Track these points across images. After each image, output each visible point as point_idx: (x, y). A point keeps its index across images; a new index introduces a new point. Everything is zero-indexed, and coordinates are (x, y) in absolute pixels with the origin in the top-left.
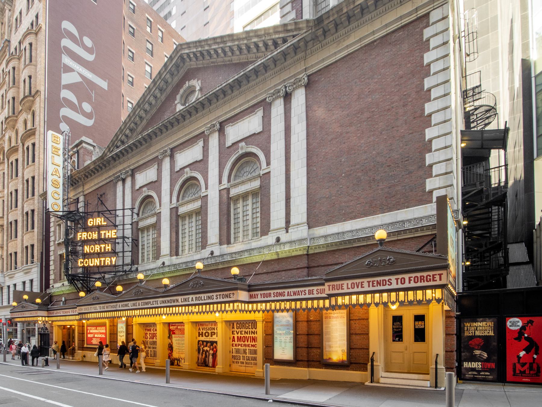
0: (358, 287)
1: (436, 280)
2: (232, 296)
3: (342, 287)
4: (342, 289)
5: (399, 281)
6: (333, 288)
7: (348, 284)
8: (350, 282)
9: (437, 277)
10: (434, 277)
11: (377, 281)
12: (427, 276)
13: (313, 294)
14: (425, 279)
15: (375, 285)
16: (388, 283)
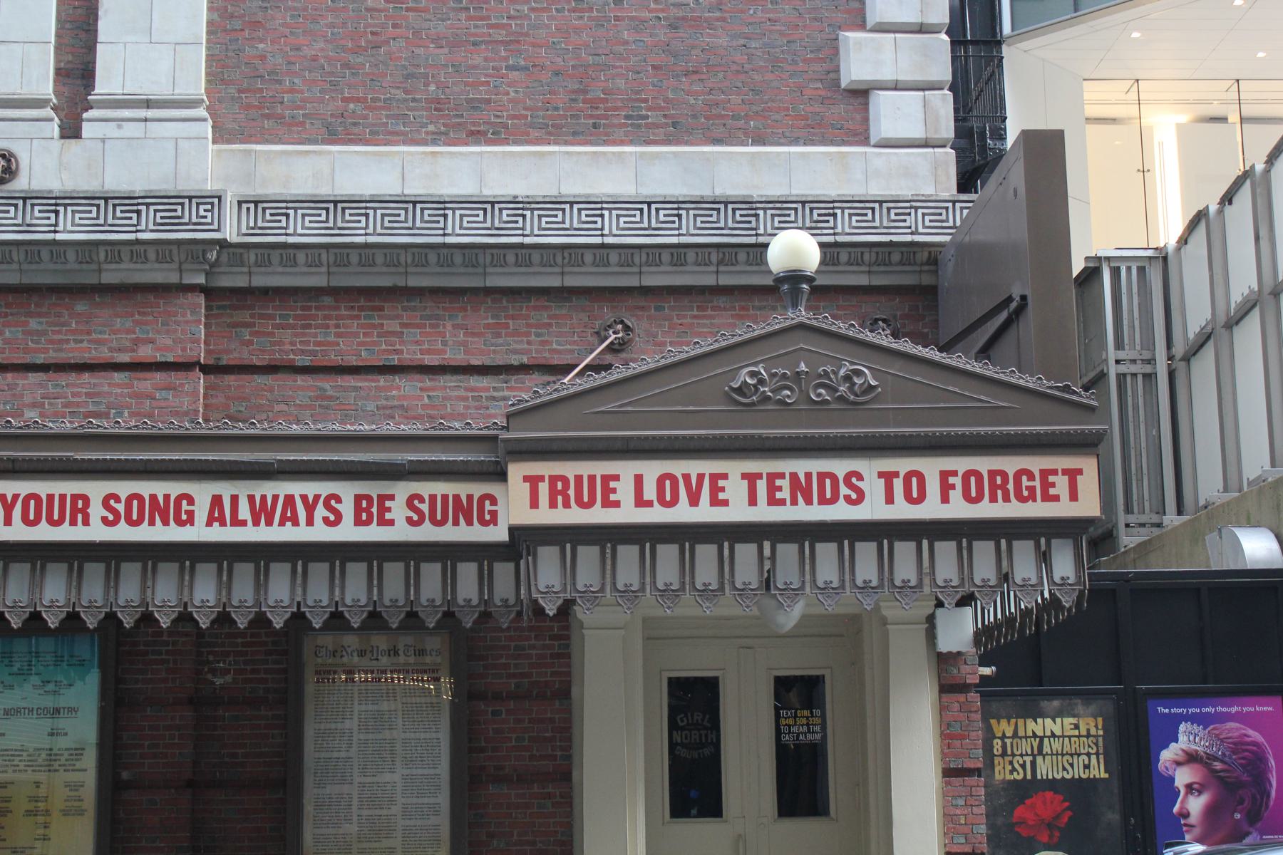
0: (694, 501)
1: (1056, 498)
3: (607, 491)
4: (607, 503)
5: (898, 484)
6: (553, 494)
7: (639, 480)
8: (652, 470)
9: (1061, 485)
10: (1046, 485)
11: (794, 476)
12: (1019, 474)
13: (383, 522)
14: (1011, 486)
15: (784, 494)
16: (844, 490)
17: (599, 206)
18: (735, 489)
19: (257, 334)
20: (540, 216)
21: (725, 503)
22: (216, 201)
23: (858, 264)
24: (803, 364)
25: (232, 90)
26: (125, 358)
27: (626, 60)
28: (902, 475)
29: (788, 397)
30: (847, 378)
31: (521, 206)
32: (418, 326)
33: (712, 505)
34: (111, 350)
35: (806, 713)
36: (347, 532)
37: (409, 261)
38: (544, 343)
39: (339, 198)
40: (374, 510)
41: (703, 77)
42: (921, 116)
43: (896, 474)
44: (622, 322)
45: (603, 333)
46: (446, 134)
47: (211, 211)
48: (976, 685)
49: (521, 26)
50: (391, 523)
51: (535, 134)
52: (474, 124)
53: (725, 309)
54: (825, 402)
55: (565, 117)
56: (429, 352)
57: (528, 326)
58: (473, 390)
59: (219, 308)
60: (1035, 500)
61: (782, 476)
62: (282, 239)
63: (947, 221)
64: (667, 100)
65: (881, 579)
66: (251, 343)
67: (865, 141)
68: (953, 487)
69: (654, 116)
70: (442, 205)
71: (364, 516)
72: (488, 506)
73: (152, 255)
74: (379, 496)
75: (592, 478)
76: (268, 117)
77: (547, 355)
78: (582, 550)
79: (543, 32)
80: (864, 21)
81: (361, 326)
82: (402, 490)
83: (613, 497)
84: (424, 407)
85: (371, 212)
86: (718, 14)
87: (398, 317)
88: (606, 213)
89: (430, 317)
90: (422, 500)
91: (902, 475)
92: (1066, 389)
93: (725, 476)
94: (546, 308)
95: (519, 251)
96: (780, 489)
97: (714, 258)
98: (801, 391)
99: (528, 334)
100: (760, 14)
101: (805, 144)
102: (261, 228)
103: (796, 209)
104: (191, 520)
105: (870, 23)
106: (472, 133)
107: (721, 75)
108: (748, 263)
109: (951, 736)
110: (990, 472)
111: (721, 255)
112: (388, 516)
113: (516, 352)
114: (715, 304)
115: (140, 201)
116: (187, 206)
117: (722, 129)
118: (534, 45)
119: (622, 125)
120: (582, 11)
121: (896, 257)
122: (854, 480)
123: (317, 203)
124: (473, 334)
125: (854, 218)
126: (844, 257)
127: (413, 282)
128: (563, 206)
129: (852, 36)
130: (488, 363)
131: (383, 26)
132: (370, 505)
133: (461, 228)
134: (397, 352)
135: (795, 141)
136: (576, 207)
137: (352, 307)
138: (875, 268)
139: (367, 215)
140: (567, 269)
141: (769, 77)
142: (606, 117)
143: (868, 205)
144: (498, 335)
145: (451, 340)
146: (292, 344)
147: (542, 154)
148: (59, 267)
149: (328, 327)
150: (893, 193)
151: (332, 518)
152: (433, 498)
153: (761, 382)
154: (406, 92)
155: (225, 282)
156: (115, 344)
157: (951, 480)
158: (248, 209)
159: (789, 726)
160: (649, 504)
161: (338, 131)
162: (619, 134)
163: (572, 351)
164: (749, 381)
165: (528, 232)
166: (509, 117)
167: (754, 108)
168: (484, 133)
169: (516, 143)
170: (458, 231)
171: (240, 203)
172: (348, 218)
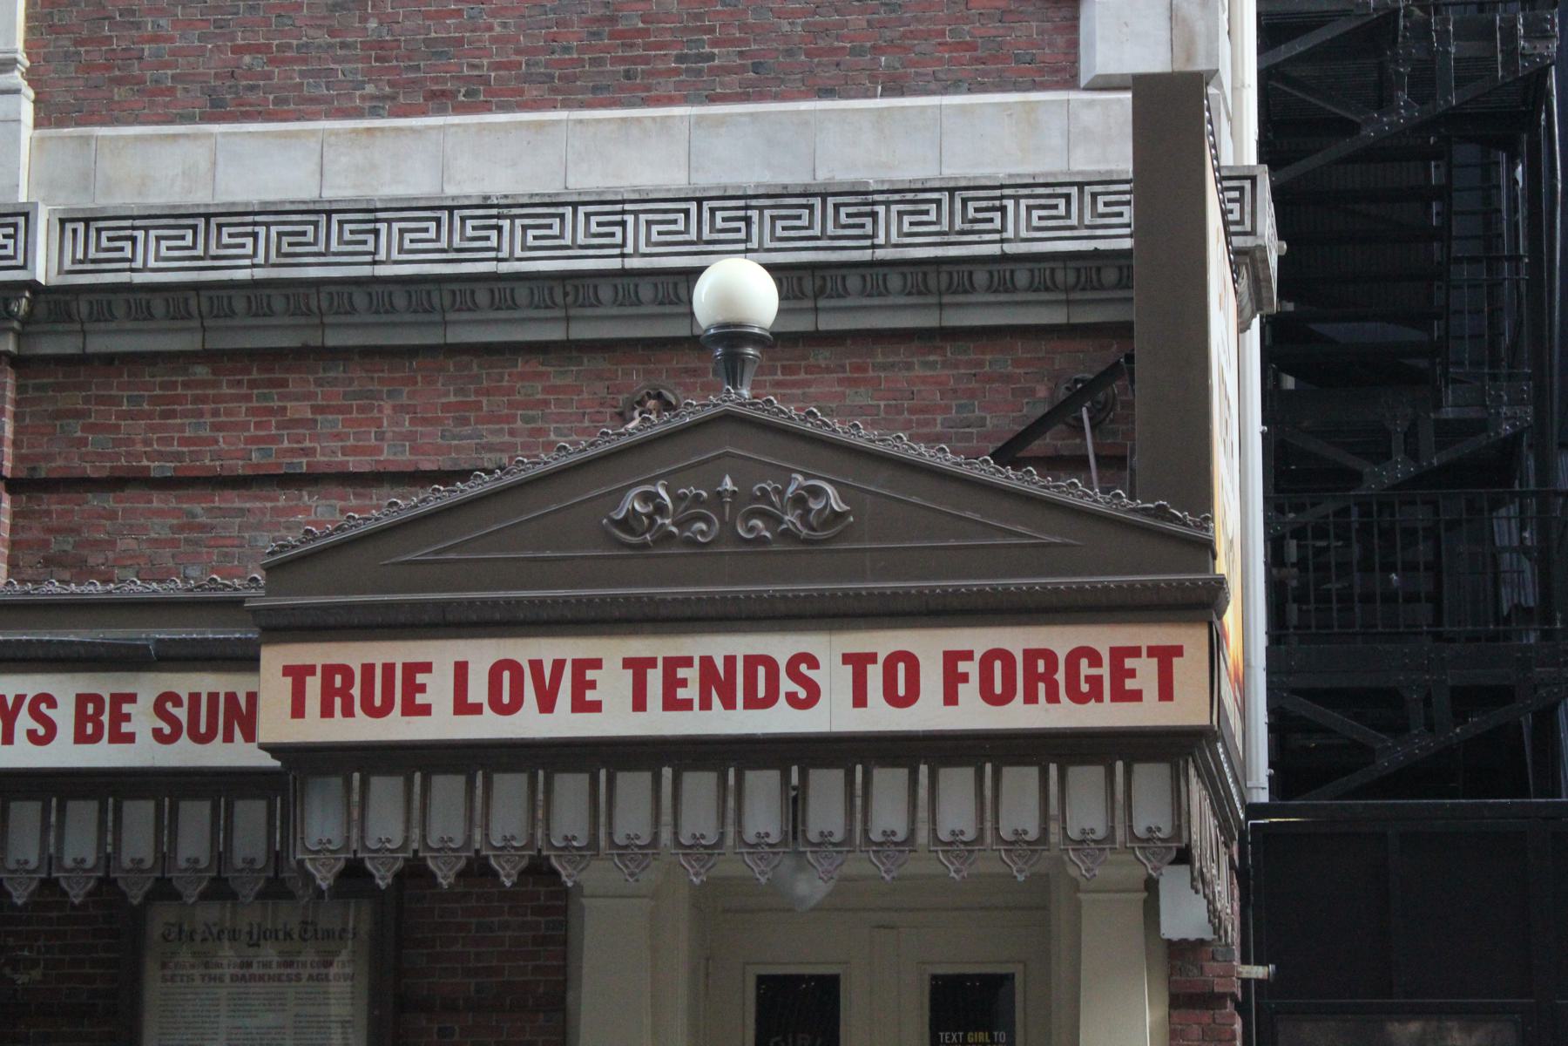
0: (547, 703)
1: (1136, 696)
3: (412, 688)
4: (411, 709)
5: (875, 674)
7: (461, 670)
8: (482, 654)
9: (1145, 673)
10: (1120, 673)
11: (707, 662)
12: (1074, 657)
13: (119, 737)
14: (1060, 677)
15: (691, 692)
16: (786, 685)
17: (618, 207)
18: (612, 685)
20: (525, 228)
21: (596, 707)
22: (21, 221)
23: (1047, 289)
25: (66, 42)
28: (881, 660)
29: (702, 533)
30: (799, 501)
31: (494, 212)
32: (339, 410)
33: (574, 710)
36: (64, 753)
37: (325, 305)
39: (212, 210)
40: (105, 718)
42: (1165, 35)
43: (872, 658)
44: (659, 396)
45: (628, 415)
46: (393, 98)
47: (14, 236)
50: (130, 738)
51: (532, 92)
52: (436, 80)
53: (828, 370)
54: (760, 540)
55: (580, 62)
56: (355, 451)
57: (511, 405)
59: (37, 388)
60: (1100, 699)
61: (687, 662)
62: (124, 278)
64: (743, 27)
65: (850, 831)
66: (83, 442)
67: (1069, 79)
68: (965, 678)
69: (723, 56)
70: (370, 215)
71: (90, 729)
74: (113, 696)
76: (119, 82)
78: (440, 782)
81: (252, 412)
82: (148, 686)
83: (420, 699)
87: (309, 396)
88: (630, 219)
90: (178, 702)
91: (881, 660)
92: (1161, 512)
93: (596, 664)
94: (541, 375)
95: (496, 286)
96: (683, 683)
98: (722, 521)
101: (970, 91)
102: (94, 261)
103: (938, 202)
106: (432, 96)
108: (864, 293)
110: (1027, 652)
111: (818, 282)
112: (126, 728)
113: (490, 448)
114: (812, 361)
117: (834, 71)
122: (803, 668)
125: (1036, 213)
126: (1022, 278)
127: (333, 339)
128: (561, 210)
132: (99, 710)
133: (401, 251)
134: (305, 452)
136: (582, 210)
137: (239, 382)
138: (1077, 296)
139: (255, 235)
140: (572, 312)
142: (646, 60)
143: (1059, 190)
144: (464, 421)
146: (147, 442)
147: (541, 125)
149: (201, 414)
151: (41, 731)
153: (661, 509)
154: (332, 33)
155: (47, 347)
157: (963, 667)
158: (75, 231)
160: (476, 709)
161: (225, 103)
162: (667, 86)
164: (637, 507)
165: (505, 254)
166: (497, 66)
167: (888, 33)
168: (453, 95)
169: (504, 108)
170: (395, 256)
171: (62, 222)
172: (226, 240)
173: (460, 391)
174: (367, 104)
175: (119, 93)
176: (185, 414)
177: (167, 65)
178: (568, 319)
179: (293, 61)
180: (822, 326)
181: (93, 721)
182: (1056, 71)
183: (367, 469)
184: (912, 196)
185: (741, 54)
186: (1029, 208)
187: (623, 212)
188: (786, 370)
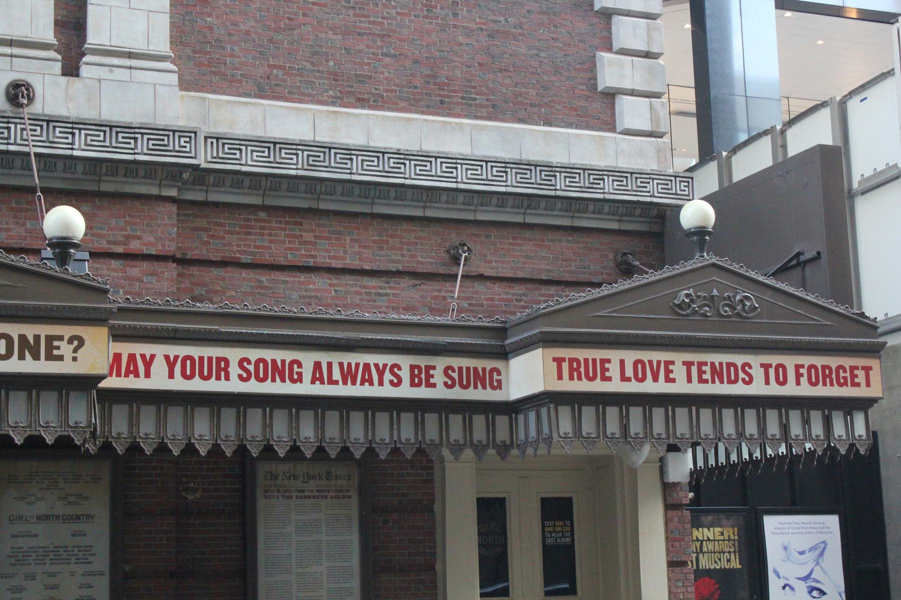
0: (656, 379)
1: (858, 385)
2: (65, 349)
3: (604, 370)
5: (772, 372)
7: (622, 362)
8: (630, 356)
10: (853, 376)
11: (713, 364)
12: (839, 367)
14: (834, 376)
15: (707, 376)
16: (741, 375)
17: (454, 161)
19: (212, 237)
20: (415, 165)
22: (193, 135)
24: (715, 291)
25: (188, 51)
26: (120, 249)
27: (461, 57)
30: (741, 301)
31: (402, 156)
32: (326, 238)
34: (109, 242)
35: (561, 523)
36: (406, 391)
37: (323, 190)
38: (412, 256)
40: (423, 376)
41: (511, 74)
42: (648, 115)
46: (341, 98)
47: (190, 142)
48: (687, 505)
49: (391, 24)
50: (434, 385)
51: (402, 104)
52: (360, 93)
53: (530, 240)
56: (334, 258)
58: (365, 287)
59: (185, 215)
61: (705, 364)
62: (237, 168)
63: (671, 189)
64: (487, 88)
66: (208, 243)
67: (613, 129)
68: (802, 375)
69: (480, 100)
70: (349, 152)
71: (416, 380)
72: (496, 377)
73: (142, 173)
74: (426, 366)
75: (594, 360)
76: (214, 73)
77: (414, 265)
79: (405, 31)
80: (611, 46)
81: (288, 236)
82: (441, 363)
83: (607, 374)
84: (332, 298)
85: (77, 132)
86: (520, 31)
87: (313, 231)
89: (333, 233)
91: (774, 366)
93: (673, 363)
94: (414, 231)
95: (399, 189)
96: (705, 372)
97: (526, 203)
99: (401, 249)
100: (546, 33)
101: (576, 128)
103: (579, 174)
104: (300, 379)
105: (616, 46)
107: (522, 74)
109: (675, 540)
110: (823, 366)
112: (432, 381)
113: (394, 261)
115: (137, 130)
116: (225, 141)
117: (524, 113)
118: (400, 40)
119: (458, 104)
120: (431, 18)
121: (638, 212)
123: (261, 143)
124: (365, 247)
125: (616, 183)
127: (323, 206)
128: (430, 159)
129: (605, 57)
130: (375, 268)
131: (296, 14)
135: (569, 125)
137: (280, 222)
140: (428, 204)
141: (553, 78)
144: (381, 249)
145: (349, 250)
146: (238, 246)
147: (409, 120)
148: (68, 176)
149: (263, 235)
150: (640, 167)
151: (395, 381)
152: (460, 369)
154: (313, 64)
156: (111, 238)
157: (801, 371)
158: (212, 143)
159: (551, 532)
160: (629, 379)
161: (266, 89)
162: (457, 110)
163: (432, 263)
166: (387, 91)
167: (544, 100)
168: (368, 100)
169: (389, 109)
171: (206, 138)
173: (379, 235)
174: (330, 100)
175: (215, 79)
176: (256, 234)
177: (237, 69)
178: (424, 207)
179: (296, 75)
180: (527, 221)
181: (419, 377)
182: (607, 124)
183: (340, 266)
184: (570, 170)
185: (487, 100)
186: (613, 181)
187: (456, 163)
188: (514, 238)
